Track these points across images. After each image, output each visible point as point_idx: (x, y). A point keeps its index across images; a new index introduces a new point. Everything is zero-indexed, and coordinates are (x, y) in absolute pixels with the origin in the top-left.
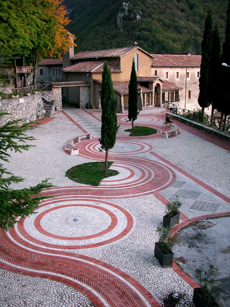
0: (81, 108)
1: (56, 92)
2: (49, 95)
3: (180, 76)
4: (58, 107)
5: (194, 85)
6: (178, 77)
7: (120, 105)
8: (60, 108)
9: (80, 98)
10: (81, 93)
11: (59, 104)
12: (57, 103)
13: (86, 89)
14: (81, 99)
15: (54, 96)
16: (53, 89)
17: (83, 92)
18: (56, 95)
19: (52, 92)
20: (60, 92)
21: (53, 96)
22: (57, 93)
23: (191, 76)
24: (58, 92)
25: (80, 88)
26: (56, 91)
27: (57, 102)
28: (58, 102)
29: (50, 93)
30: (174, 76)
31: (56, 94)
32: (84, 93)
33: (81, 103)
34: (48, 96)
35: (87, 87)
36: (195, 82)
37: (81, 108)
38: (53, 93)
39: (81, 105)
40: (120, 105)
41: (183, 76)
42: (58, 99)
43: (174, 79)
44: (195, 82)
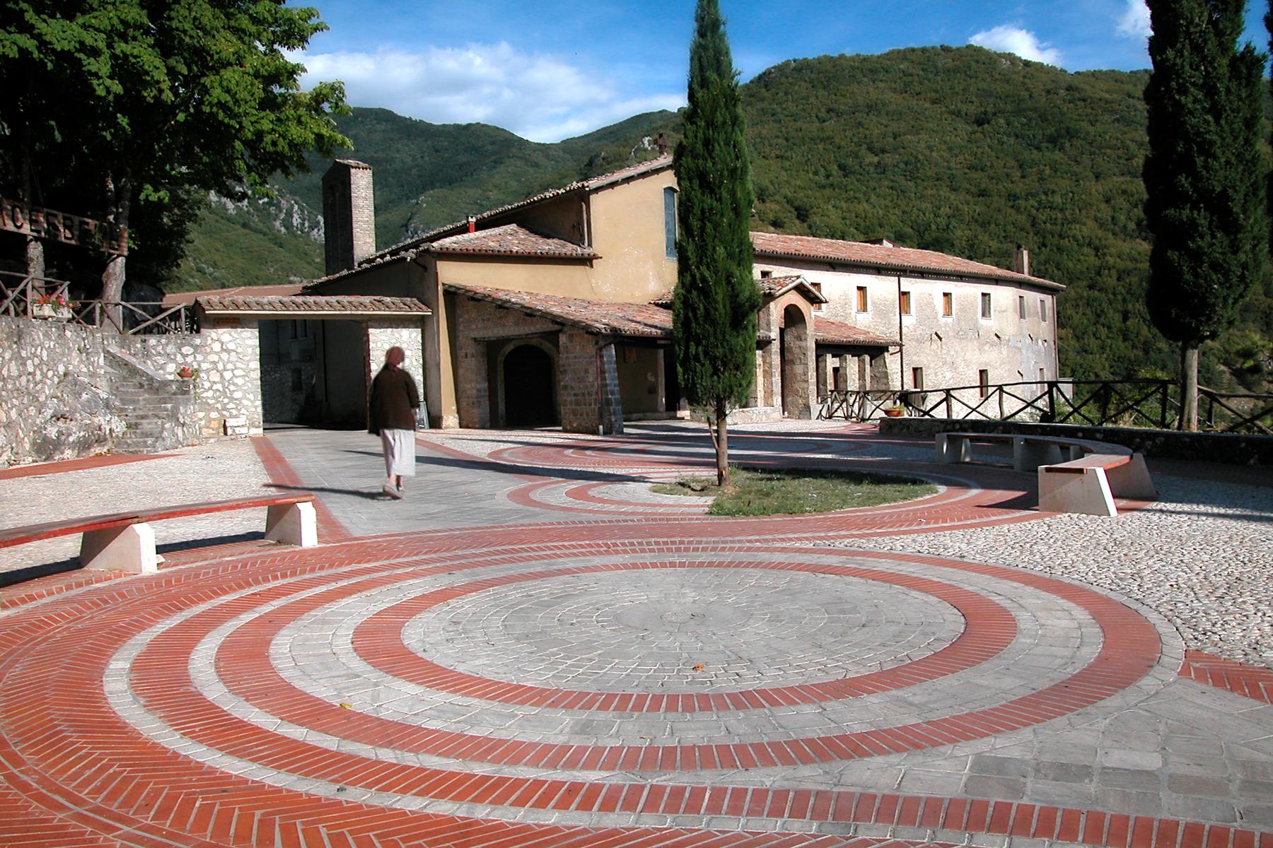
2: (185, 356)
3: (874, 303)
4: (236, 417)
5: (934, 346)
6: (864, 309)
8: (253, 425)
11: (245, 402)
12: (232, 399)
15: (214, 363)
18: (225, 356)
19: (198, 341)
23: (921, 309)
24: (238, 345)
27: (232, 392)
28: (237, 395)
29: (192, 346)
30: (845, 304)
31: (228, 351)
36: (936, 334)
41: (885, 305)
42: (240, 381)
43: (847, 316)
44: (936, 334)
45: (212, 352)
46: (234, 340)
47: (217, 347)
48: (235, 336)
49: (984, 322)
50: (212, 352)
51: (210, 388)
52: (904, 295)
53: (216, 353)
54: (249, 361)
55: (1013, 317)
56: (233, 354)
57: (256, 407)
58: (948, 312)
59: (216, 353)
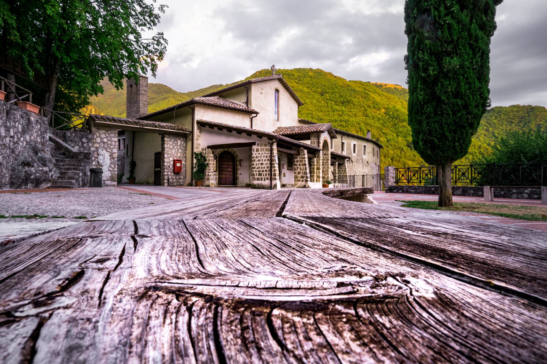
0: (166, 184)
1: (101, 138)
5: (351, 164)
7: (271, 171)
9: (164, 162)
10: (168, 150)
13: (179, 142)
14: (166, 164)
16: (94, 129)
17: (171, 147)
18: (102, 145)
19: (90, 136)
20: (113, 139)
21: (93, 146)
22: (105, 140)
23: (347, 150)
24: (108, 140)
25: (166, 139)
26: (103, 136)
29: (87, 138)
31: (104, 143)
32: (174, 151)
33: (166, 173)
34: (78, 145)
35: (182, 139)
37: (166, 184)
38: (92, 139)
39: (166, 177)
40: (271, 171)
45: (96, 142)
46: (107, 137)
47: (98, 140)
48: (107, 135)
49: (364, 157)
50: (96, 142)
51: (94, 160)
52: (343, 143)
53: (98, 143)
54: (113, 148)
55: (371, 155)
56: (106, 144)
57: (115, 171)
58: (354, 152)
59: (98, 143)
